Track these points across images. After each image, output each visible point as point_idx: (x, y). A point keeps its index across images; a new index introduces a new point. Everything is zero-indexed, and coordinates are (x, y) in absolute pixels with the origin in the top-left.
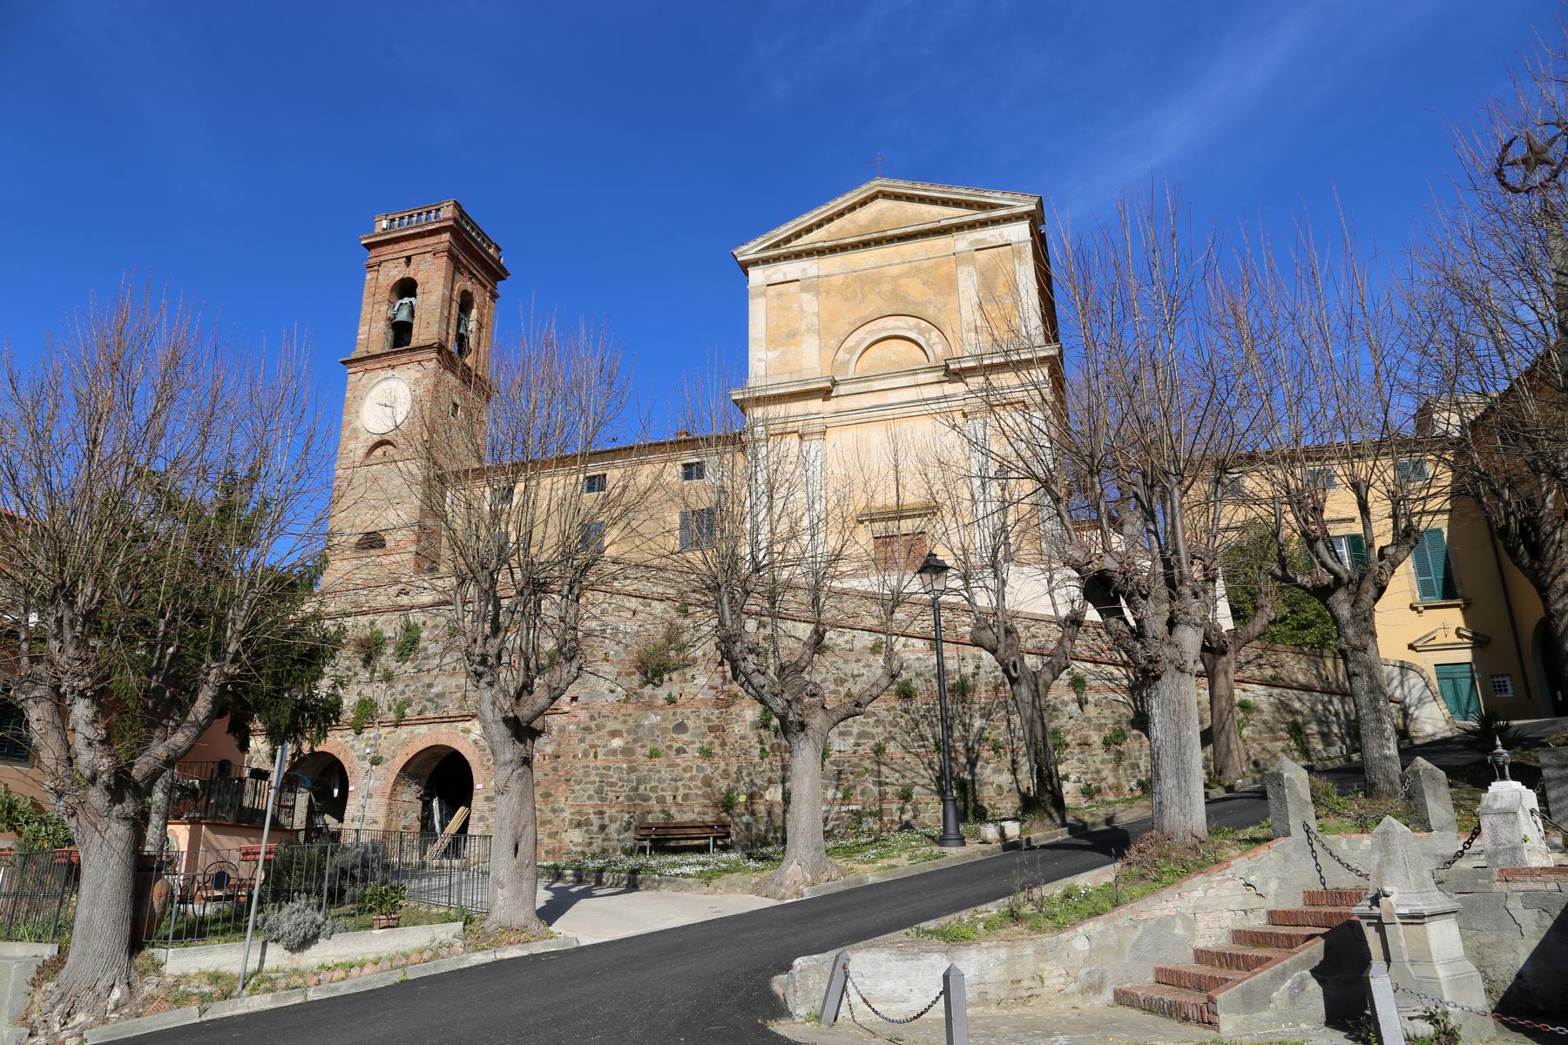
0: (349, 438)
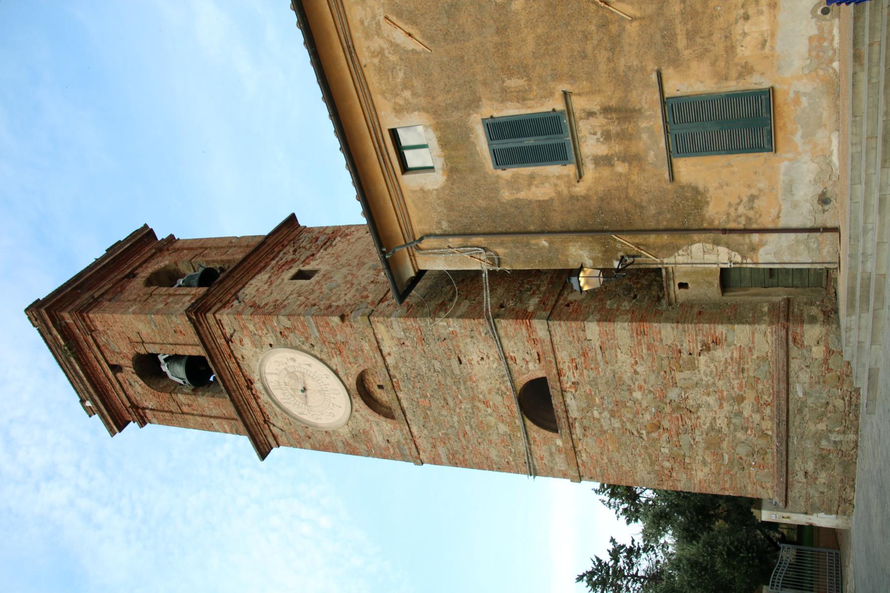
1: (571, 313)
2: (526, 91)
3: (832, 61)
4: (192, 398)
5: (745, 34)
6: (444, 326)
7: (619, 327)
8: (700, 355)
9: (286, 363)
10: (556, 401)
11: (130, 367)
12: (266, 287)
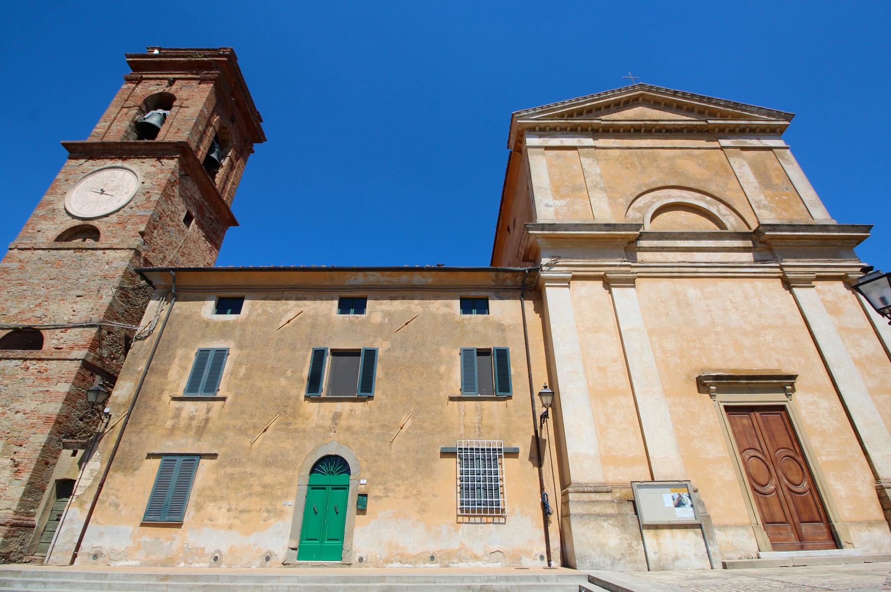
0: (44, 218)
1: (83, 376)
2: (236, 376)
3: (185, 562)
4: (131, 119)
5: (220, 508)
6: (108, 293)
7: (58, 406)
8: (11, 459)
9: (127, 187)
10: (20, 353)
11: (169, 90)
12: (188, 194)
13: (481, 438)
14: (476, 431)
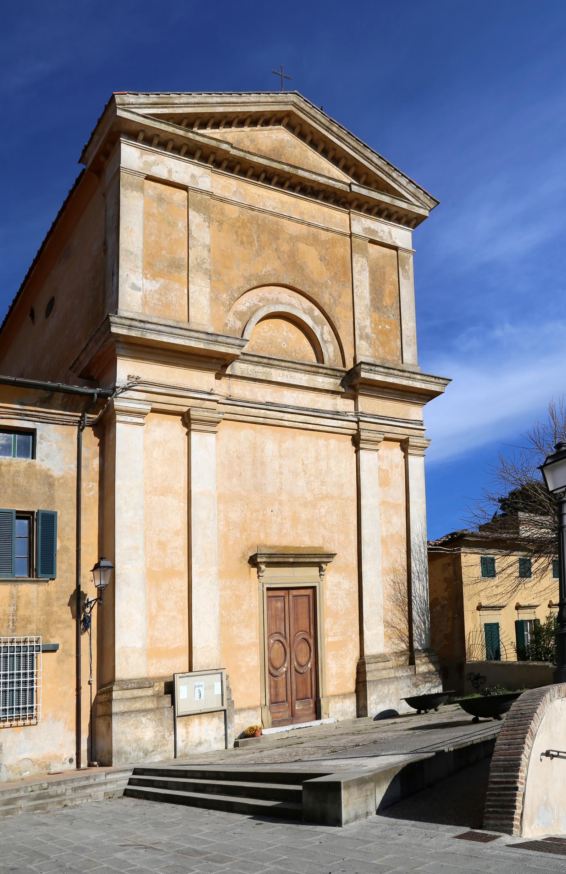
13: (15, 634)
14: (9, 626)
